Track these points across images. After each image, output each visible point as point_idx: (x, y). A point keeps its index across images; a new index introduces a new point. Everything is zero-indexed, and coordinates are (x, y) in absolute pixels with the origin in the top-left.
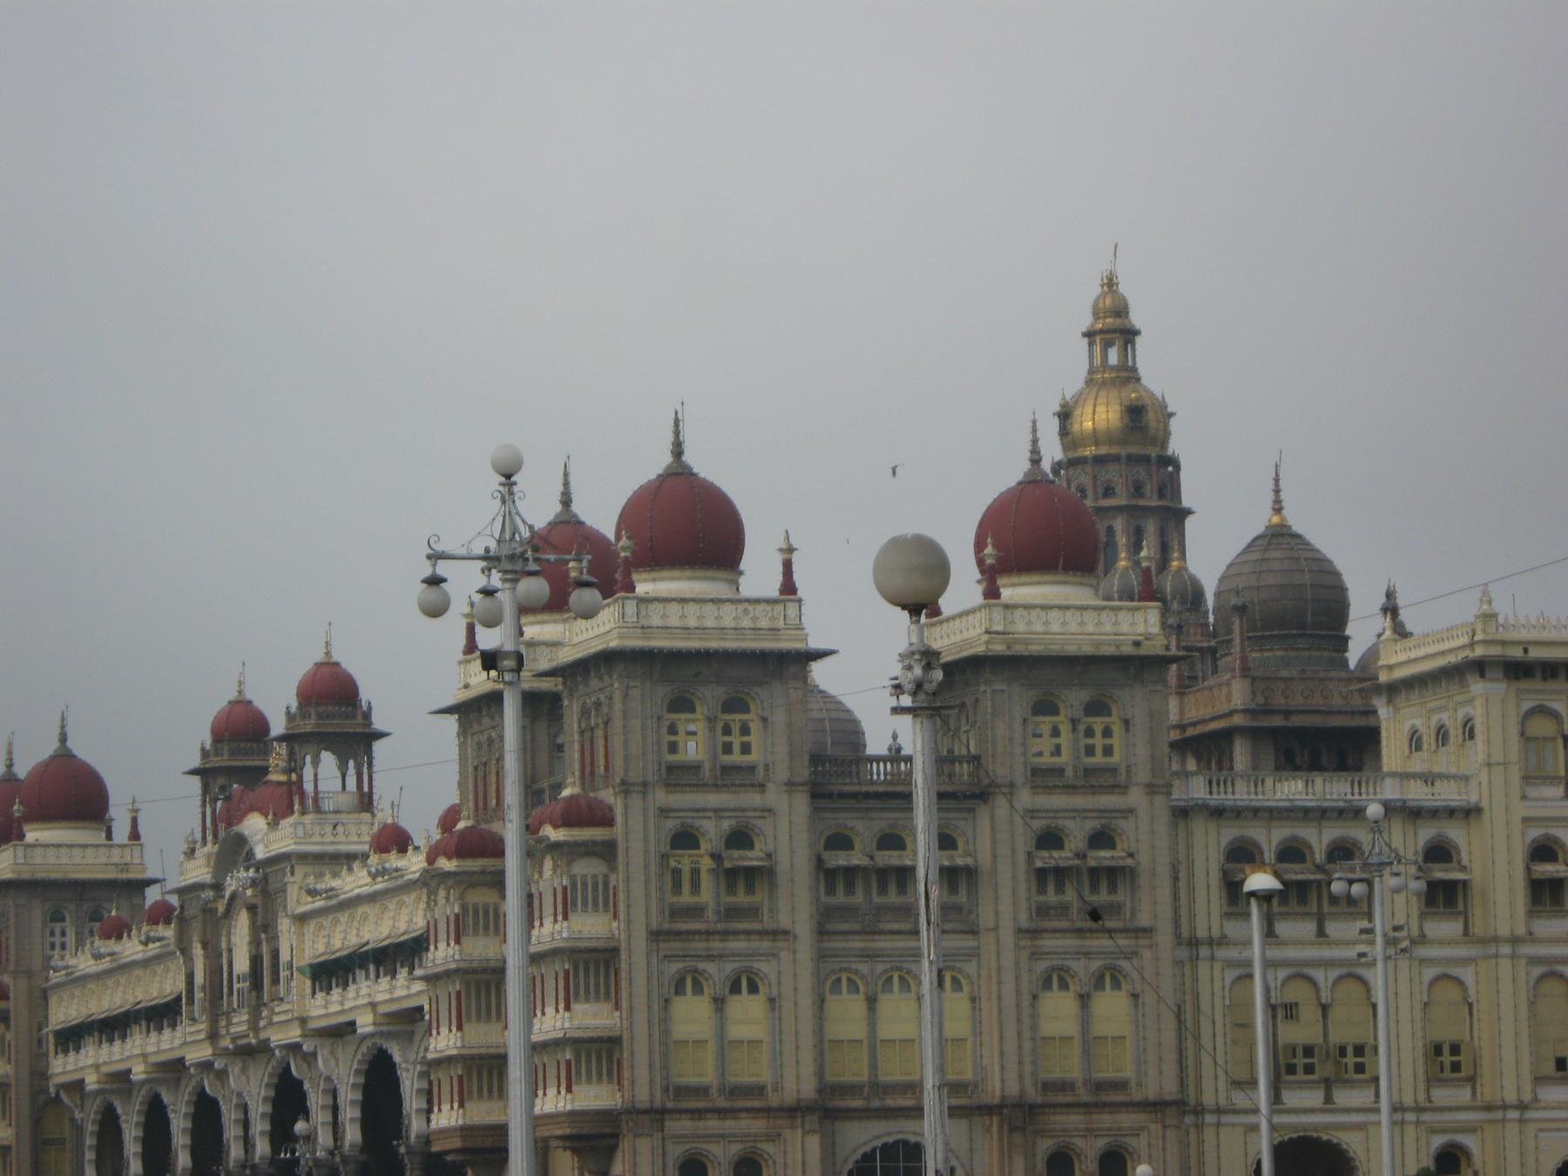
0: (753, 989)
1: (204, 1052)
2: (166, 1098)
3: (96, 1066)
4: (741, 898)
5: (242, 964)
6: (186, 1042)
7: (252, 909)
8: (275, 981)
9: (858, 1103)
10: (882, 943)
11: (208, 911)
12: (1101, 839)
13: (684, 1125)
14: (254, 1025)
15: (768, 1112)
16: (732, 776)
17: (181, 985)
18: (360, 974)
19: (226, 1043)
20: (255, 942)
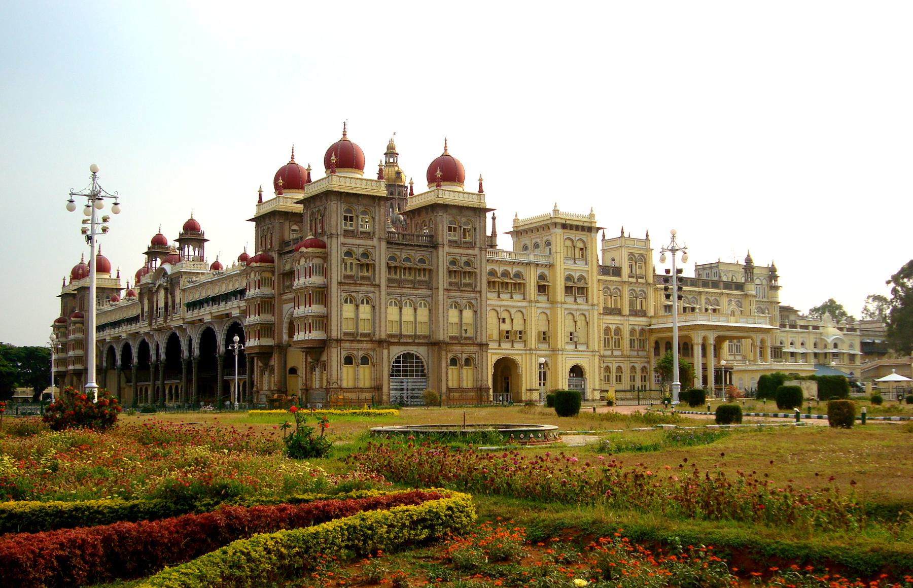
0: (368, 303)
1: (148, 329)
4: (365, 274)
5: (162, 304)
6: (142, 327)
7: (166, 289)
8: (174, 308)
11: (150, 290)
12: (467, 263)
13: (347, 345)
14: (165, 321)
15: (372, 341)
17: (140, 312)
18: (205, 305)
19: (155, 327)
20: (166, 298)
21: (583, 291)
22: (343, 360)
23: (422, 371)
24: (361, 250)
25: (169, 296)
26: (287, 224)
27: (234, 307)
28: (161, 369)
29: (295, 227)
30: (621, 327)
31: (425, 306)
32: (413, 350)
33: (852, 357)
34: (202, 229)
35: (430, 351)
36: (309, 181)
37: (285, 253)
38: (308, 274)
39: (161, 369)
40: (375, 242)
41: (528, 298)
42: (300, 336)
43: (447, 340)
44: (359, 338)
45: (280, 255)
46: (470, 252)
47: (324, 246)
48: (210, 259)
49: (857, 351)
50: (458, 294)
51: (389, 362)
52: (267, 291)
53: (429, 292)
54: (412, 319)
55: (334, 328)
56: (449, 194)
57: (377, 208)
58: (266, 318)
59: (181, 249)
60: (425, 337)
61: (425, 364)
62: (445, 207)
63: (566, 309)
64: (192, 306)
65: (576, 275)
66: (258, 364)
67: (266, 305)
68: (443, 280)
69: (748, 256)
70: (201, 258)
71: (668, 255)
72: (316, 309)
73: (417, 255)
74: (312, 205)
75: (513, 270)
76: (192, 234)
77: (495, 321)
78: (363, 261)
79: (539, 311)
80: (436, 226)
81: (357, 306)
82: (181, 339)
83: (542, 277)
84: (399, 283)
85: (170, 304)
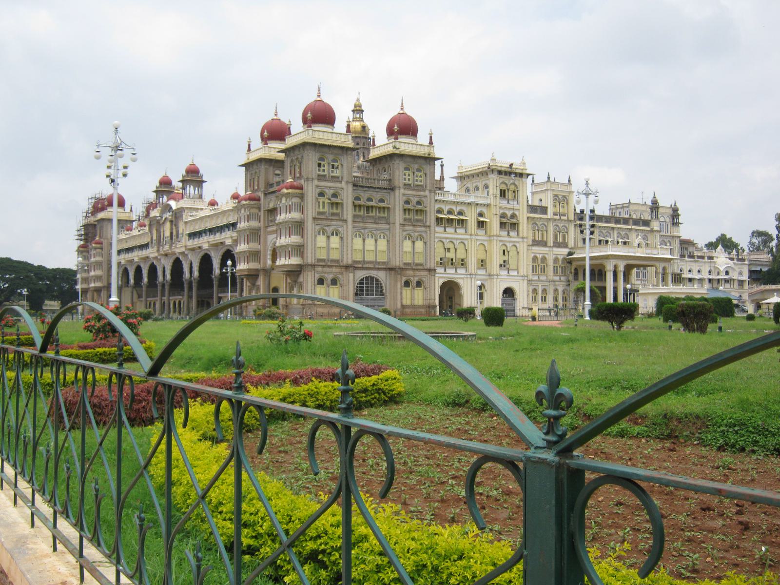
0: (337, 235)
1: (156, 255)
2: (129, 269)
3: (124, 259)
4: (335, 211)
5: (167, 234)
6: (151, 252)
7: (171, 221)
8: (177, 237)
9: (360, 266)
10: (368, 225)
12: (419, 203)
13: (320, 269)
15: (340, 266)
16: (335, 179)
17: (149, 240)
18: (204, 235)
19: (163, 253)
20: (172, 229)
21: (514, 226)
22: (316, 281)
23: (381, 291)
24: (332, 192)
25: (174, 227)
26: (271, 169)
27: (227, 237)
28: (167, 288)
29: (278, 172)
30: (546, 256)
31: (384, 238)
32: (373, 273)
33: (741, 283)
34: (201, 172)
35: (388, 275)
36: (290, 134)
37: (269, 193)
38: (288, 210)
39: (167, 288)
40: (343, 185)
41: (469, 232)
42: (281, 261)
43: (402, 266)
44: (329, 264)
45: (265, 194)
46: (422, 193)
47: (301, 188)
48: (207, 198)
49: (745, 277)
50: (411, 228)
51: (354, 283)
52: (254, 224)
53: (387, 226)
54: (373, 248)
55: (309, 255)
56: (406, 145)
57: (345, 156)
58: (254, 246)
59: (184, 188)
60: (384, 263)
61: (383, 285)
62: (401, 156)
63: (501, 241)
64: (193, 235)
65: (509, 213)
66: (247, 284)
67: (254, 235)
68: (398, 216)
69: (654, 197)
70: (201, 197)
71: (583, 197)
72: (295, 239)
73: (377, 195)
74: (292, 154)
75: (457, 209)
76: (193, 177)
77: (442, 250)
78: (334, 200)
79: (478, 243)
80: (393, 172)
81: (328, 237)
82: (184, 262)
83: (481, 215)
84: (363, 220)
85: (174, 233)
